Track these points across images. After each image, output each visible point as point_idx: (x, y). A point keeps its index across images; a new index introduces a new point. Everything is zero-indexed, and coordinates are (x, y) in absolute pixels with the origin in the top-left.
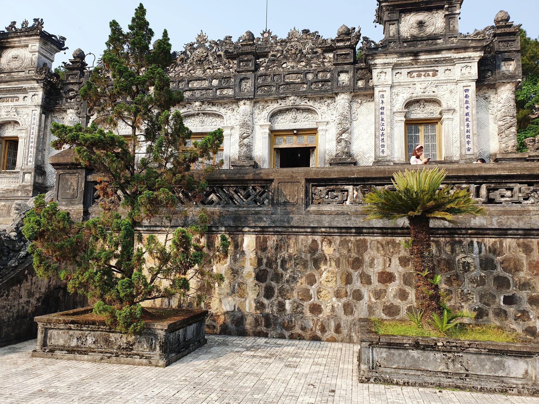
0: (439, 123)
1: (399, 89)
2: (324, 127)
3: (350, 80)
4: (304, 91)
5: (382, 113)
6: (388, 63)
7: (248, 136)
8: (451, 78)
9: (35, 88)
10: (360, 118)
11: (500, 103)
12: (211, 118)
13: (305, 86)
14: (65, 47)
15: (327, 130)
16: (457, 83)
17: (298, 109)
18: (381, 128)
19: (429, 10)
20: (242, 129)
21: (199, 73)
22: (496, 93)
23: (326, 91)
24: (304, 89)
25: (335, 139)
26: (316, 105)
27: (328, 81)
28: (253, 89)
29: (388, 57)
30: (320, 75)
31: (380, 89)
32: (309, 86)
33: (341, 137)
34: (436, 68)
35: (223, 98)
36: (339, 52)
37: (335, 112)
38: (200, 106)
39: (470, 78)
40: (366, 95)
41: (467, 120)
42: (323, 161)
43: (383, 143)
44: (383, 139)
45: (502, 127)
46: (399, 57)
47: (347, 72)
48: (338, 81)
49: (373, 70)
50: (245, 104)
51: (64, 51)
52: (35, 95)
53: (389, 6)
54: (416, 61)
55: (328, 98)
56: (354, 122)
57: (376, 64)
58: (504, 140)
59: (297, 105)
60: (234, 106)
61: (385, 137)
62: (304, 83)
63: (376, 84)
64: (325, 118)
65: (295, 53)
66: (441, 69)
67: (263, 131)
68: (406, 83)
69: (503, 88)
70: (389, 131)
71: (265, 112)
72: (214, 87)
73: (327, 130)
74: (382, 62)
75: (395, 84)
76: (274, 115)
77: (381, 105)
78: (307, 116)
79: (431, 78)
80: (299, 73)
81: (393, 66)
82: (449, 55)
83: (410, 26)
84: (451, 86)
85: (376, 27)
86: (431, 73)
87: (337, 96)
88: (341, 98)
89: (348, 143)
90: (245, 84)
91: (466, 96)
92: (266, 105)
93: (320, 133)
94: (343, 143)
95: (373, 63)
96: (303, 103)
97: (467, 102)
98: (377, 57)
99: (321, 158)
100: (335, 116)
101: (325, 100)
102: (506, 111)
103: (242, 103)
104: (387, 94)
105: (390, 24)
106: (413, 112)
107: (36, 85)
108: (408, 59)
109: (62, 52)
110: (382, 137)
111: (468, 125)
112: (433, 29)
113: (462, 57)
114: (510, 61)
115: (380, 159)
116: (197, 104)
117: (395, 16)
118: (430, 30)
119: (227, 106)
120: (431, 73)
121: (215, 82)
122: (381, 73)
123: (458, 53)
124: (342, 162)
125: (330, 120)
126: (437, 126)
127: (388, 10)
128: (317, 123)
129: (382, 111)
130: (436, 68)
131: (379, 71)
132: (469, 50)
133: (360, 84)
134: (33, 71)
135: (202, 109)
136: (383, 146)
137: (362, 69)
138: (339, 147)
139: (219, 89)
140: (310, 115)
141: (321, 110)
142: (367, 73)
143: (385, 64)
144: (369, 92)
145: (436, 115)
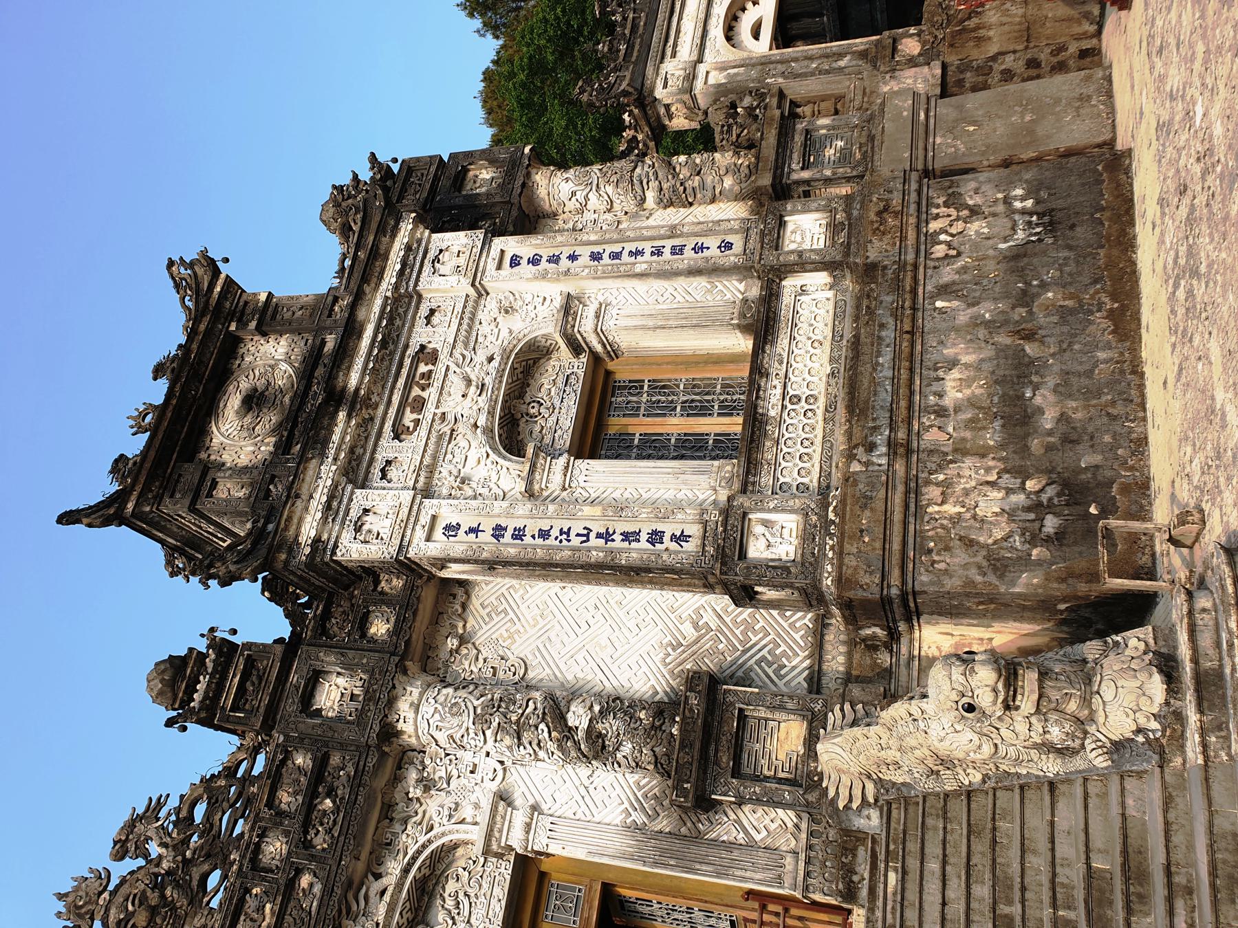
0: (611, 366)
1: (445, 473)
2: (519, 818)
3: (350, 668)
4: (323, 891)
5: (519, 534)
6: (331, 498)
8: (459, 308)
10: (521, 648)
11: (587, 198)
13: (305, 880)
15: (535, 808)
16: (482, 293)
18: (576, 541)
19: (222, 375)
22: (555, 215)
23: (356, 781)
24: (317, 889)
25: (583, 771)
26: (411, 840)
27: (321, 763)
29: (304, 492)
30: (285, 798)
31: (420, 534)
32: (312, 858)
33: (581, 734)
34: (411, 351)
36: (228, 700)
37: (467, 757)
39: (477, 250)
40: (437, 617)
41: (616, 256)
42: (677, 845)
43: (644, 537)
44: (626, 536)
45: (665, 186)
46: (323, 455)
47: (315, 678)
48: (340, 719)
49: (339, 556)
53: (146, 489)
54: (358, 403)
55: (397, 778)
56: (531, 674)
57: (317, 541)
58: (709, 179)
61: (621, 527)
62: (291, 884)
63: (393, 551)
64: (477, 806)
65: (153, 911)
66: (421, 335)
68: (431, 446)
69: (542, 192)
70: (597, 511)
73: (535, 808)
74: (319, 515)
75: (420, 485)
77: (486, 537)
78: (450, 903)
79: (440, 369)
80: (242, 901)
81: (350, 481)
82: (378, 302)
83: (245, 434)
84: (489, 308)
86: (423, 368)
87: (398, 734)
88: (410, 715)
89: (613, 704)
91: (534, 261)
93: (540, 842)
94: (611, 726)
95: (308, 550)
97: (554, 259)
98: (292, 532)
99: (663, 852)
100: (480, 759)
101: (398, 796)
102: (614, 178)
104: (448, 513)
105: (210, 495)
106: (548, 440)
108: (342, 428)
110: (618, 537)
111: (637, 253)
112: (284, 366)
113: (398, 267)
114: (464, 178)
115: (710, 550)
117: (190, 474)
118: (284, 375)
120: (423, 368)
122: (358, 529)
123: (380, 278)
124: (697, 736)
125: (494, 786)
126: (623, 373)
127: (159, 499)
128: (487, 852)
129: (508, 534)
130: (411, 351)
131: (347, 536)
132: (382, 248)
133: (380, 628)
136: (656, 537)
137: (326, 615)
138: (627, 748)
140: (451, 886)
141: (437, 819)
142: (352, 596)
143: (328, 507)
144: (428, 595)
145: (579, 366)
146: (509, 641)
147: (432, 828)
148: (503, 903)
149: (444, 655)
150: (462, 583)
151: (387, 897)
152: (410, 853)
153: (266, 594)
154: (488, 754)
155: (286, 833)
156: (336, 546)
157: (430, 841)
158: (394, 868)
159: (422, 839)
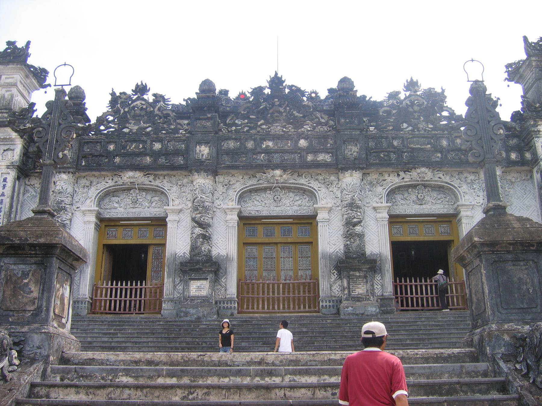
2: (469, 213)
7: (360, 222)
9: (11, 140)
12: (291, 194)
14: (46, 83)
17: (425, 186)
20: (350, 212)
21: (277, 128)
24: (437, 159)
28: (364, 156)
35: (317, 165)
38: (281, 176)
50: (351, 175)
51: (45, 90)
52: (7, 150)
59: (427, 181)
60: (333, 178)
67: (379, 215)
71: (379, 189)
72: (304, 150)
76: (392, 193)
85: (508, 86)
90: (350, 147)
92: (381, 178)
95: (536, 130)
96: (437, 179)
101: (466, 175)
103: (347, 174)
107: (14, 135)
109: (42, 90)
116: (278, 172)
119: (321, 178)
121: (303, 143)
134: (6, 115)
135: (282, 181)
139: (311, 153)
140: (442, 195)
146: (517, 198)
147: (460, 187)
148: (443, 213)
149: (508, 178)
150: (532, 177)
151: (439, 179)
152: (451, 183)
153: (514, 113)
154: (483, 199)
155: (449, 145)
156: (538, 137)
157: (456, 188)
158: (447, 179)
159: (456, 185)
